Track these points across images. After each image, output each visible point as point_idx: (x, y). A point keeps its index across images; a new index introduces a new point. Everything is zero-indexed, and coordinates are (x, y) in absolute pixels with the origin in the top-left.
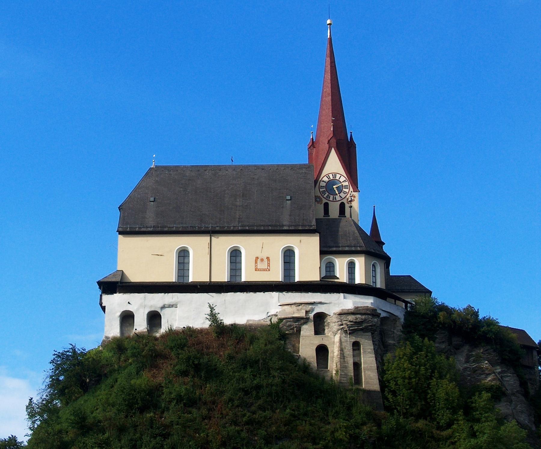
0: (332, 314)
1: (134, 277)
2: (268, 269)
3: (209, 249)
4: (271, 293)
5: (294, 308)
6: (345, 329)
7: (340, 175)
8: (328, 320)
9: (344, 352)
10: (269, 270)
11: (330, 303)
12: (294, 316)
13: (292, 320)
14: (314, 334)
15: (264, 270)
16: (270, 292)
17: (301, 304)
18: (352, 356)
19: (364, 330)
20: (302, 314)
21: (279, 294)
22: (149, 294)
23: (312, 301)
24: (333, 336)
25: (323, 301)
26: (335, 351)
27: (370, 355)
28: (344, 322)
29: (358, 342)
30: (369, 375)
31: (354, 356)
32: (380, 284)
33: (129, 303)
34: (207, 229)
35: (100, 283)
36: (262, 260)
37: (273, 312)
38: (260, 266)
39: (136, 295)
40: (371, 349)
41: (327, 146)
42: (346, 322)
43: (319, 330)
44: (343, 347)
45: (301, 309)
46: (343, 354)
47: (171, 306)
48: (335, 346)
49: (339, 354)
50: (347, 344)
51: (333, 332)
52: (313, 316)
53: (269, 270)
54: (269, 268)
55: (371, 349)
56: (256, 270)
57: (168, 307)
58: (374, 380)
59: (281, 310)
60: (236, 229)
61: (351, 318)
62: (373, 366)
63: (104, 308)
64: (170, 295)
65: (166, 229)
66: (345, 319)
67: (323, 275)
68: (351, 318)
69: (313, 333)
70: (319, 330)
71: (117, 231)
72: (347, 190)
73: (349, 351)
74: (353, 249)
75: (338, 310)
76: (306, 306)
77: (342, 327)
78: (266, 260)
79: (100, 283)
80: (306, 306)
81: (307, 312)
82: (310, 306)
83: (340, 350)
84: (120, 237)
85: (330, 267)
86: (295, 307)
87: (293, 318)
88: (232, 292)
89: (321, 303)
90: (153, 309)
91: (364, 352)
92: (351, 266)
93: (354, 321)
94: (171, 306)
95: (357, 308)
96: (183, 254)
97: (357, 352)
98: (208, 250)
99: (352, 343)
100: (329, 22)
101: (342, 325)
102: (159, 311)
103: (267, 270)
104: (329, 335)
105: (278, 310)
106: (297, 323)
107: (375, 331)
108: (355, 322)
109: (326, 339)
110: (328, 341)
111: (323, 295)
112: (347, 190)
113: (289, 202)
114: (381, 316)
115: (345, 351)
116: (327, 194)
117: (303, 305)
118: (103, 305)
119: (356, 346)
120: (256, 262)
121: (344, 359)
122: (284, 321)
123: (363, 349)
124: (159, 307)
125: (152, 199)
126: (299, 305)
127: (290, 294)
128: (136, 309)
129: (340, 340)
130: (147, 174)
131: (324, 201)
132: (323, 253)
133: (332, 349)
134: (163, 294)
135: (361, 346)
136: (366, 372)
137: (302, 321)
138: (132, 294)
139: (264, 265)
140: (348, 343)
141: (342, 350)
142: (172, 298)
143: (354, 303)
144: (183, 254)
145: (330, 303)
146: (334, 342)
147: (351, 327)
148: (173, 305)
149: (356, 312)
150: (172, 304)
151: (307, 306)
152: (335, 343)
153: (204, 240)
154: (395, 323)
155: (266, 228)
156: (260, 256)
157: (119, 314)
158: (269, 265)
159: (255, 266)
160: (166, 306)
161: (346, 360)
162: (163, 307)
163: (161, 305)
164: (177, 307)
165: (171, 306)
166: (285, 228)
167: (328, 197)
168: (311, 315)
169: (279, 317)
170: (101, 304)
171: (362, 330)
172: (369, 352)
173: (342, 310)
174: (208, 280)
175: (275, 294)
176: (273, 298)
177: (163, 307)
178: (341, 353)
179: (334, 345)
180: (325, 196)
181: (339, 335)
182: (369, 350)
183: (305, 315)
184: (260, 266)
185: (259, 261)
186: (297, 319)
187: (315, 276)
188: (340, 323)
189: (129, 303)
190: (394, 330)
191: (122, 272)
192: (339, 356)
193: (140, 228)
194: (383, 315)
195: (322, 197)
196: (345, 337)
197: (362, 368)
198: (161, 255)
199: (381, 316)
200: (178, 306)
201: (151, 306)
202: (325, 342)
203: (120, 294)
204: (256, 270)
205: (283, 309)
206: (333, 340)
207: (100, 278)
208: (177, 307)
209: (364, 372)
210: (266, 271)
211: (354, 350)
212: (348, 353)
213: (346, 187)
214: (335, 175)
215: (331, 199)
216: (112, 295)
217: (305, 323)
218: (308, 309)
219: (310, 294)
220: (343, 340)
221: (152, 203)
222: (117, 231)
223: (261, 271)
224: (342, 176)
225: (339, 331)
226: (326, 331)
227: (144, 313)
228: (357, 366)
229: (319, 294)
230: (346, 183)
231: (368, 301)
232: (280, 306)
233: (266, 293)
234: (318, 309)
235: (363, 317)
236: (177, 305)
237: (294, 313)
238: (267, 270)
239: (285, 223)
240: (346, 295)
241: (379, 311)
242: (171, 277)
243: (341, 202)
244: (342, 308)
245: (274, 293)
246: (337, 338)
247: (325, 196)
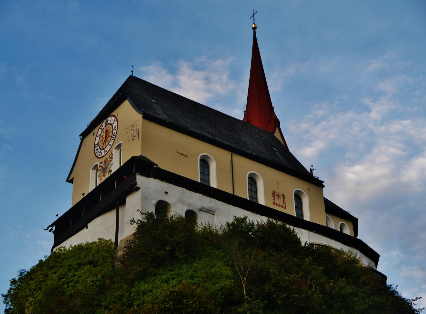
2: (284, 206)
4: (300, 229)
15: (281, 206)
33: (166, 193)
36: (278, 196)
39: (174, 186)
54: (285, 205)
56: (274, 203)
78: (282, 197)
90: (191, 208)
120: (273, 196)
127: (317, 235)
142: (211, 203)
148: (210, 211)
150: (210, 209)
153: (226, 155)
156: (277, 191)
157: (155, 202)
158: (284, 203)
160: (204, 209)
162: (201, 210)
163: (199, 206)
164: (214, 214)
165: (208, 211)
184: (277, 201)
185: (276, 196)
189: (166, 193)
198: (185, 156)
200: (216, 213)
208: (214, 214)
210: (283, 208)
223: (278, 206)
227: (182, 209)
236: (214, 212)
238: (284, 207)
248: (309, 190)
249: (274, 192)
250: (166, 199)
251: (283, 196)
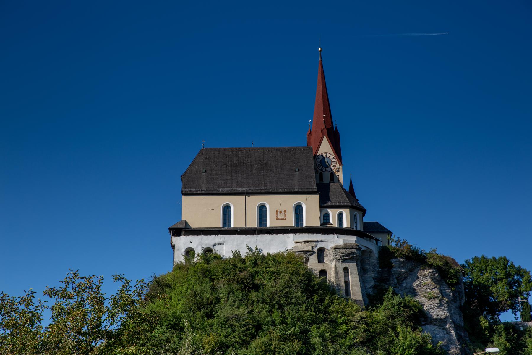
0: (329, 249)
1: (194, 225)
3: (245, 205)
4: (288, 234)
5: (304, 245)
6: (338, 259)
7: (330, 154)
8: (326, 252)
9: (339, 274)
10: (286, 219)
11: (328, 241)
12: (304, 250)
13: (302, 252)
14: (317, 262)
15: (282, 219)
16: (288, 234)
17: (308, 242)
18: (344, 277)
19: (351, 260)
20: (310, 249)
21: (293, 235)
22: (205, 236)
23: (316, 239)
24: (330, 264)
25: (323, 239)
26: (332, 274)
27: (355, 276)
28: (338, 254)
29: (348, 267)
30: (355, 289)
31: (345, 277)
32: (360, 228)
33: (191, 242)
34: (243, 192)
35: (170, 229)
36: (281, 212)
37: (289, 248)
38: (279, 216)
39: (196, 237)
40: (356, 272)
41: (321, 134)
42: (339, 253)
43: (320, 260)
44: (338, 271)
45: (309, 245)
46: (338, 275)
47: (219, 244)
48: (332, 270)
49: (335, 275)
50: (340, 269)
51: (330, 261)
52: (316, 250)
53: (286, 219)
54: (285, 217)
55: (356, 272)
56: (277, 219)
57: (218, 245)
58: (358, 293)
59: (295, 246)
60: (263, 191)
61: (343, 251)
62: (357, 283)
63: (173, 247)
64: (219, 236)
65: (215, 192)
66: (338, 252)
67: (322, 222)
68: (343, 251)
69: (317, 261)
70: (320, 260)
71: (181, 193)
72: (335, 164)
73: (342, 274)
74: (342, 204)
75: (333, 245)
76: (312, 243)
77: (336, 257)
79: (170, 229)
80: (312, 243)
81: (312, 248)
82: (315, 243)
83: (336, 273)
84: (183, 196)
85: (326, 217)
86: (305, 244)
87: (303, 251)
88: (261, 234)
89: (322, 241)
90: (207, 246)
91: (351, 274)
92: (340, 216)
93: (345, 253)
94: (219, 244)
95: (346, 244)
96: (227, 209)
97: (346, 274)
98: (244, 206)
99: (343, 268)
100: (320, 49)
101: (336, 256)
102: (212, 247)
103: (285, 219)
104: (328, 262)
105: (293, 246)
106: (306, 255)
107: (358, 259)
108: (346, 254)
109: (326, 265)
110: (327, 266)
111: (323, 235)
112: (335, 164)
113: (297, 173)
114: (362, 250)
115: (339, 273)
116: (322, 167)
117: (310, 242)
118: (173, 244)
119: (346, 269)
120: (277, 214)
121: (338, 279)
122: (310, 253)
123: (351, 272)
124: (212, 245)
125: (204, 171)
126: (307, 243)
127: (301, 235)
128: (196, 246)
129: (336, 266)
130: (199, 153)
131: (320, 172)
132: (322, 207)
133: (330, 272)
134: (214, 236)
135: (349, 270)
136: (353, 287)
137: (310, 253)
138: (193, 236)
139: (282, 216)
140: (341, 268)
141: (337, 273)
142: (221, 239)
143: (344, 240)
144: (227, 209)
145: (328, 241)
146: (331, 267)
147: (342, 257)
148: (221, 243)
149: (346, 247)
151: (313, 243)
152: (332, 268)
154: (370, 254)
155: (283, 191)
156: (280, 209)
158: (285, 215)
159: (276, 216)
160: (216, 244)
161: (339, 280)
162: (214, 245)
163: (213, 243)
164: (224, 245)
166: (297, 190)
167: (322, 169)
168: (315, 249)
169: (294, 251)
170: (171, 244)
171: (350, 259)
172: (355, 274)
173: (336, 246)
174: (245, 226)
175: (291, 236)
176: (289, 238)
177: (214, 245)
178: (336, 275)
179: (331, 269)
180: (320, 168)
181: (335, 263)
182: (355, 273)
183: (311, 249)
184: (279, 216)
186: (307, 252)
187: (316, 223)
188: (335, 254)
189: (191, 242)
190: (369, 259)
191: (185, 221)
192: (335, 277)
193: (197, 191)
194: (363, 248)
195: (317, 169)
196: (339, 264)
197: (350, 285)
198: (212, 209)
199: (362, 250)
201: (206, 245)
202: (325, 267)
203: (185, 236)
204: (277, 219)
205: (296, 245)
206: (330, 266)
207: (170, 226)
209: (352, 287)
211: (345, 273)
212: (341, 275)
213: (334, 162)
214: (327, 154)
215: (324, 170)
216: (179, 237)
217: (311, 255)
218: (313, 245)
219: (314, 235)
220: (337, 266)
221: (204, 173)
222: (181, 193)
223: (280, 219)
224: (331, 155)
225: (335, 260)
226: (325, 260)
228: (347, 283)
229: (320, 235)
230: (334, 160)
231: (352, 239)
232: (295, 244)
233: (284, 234)
234: (320, 245)
235: (351, 250)
237: (303, 248)
238: (285, 219)
239: (296, 187)
240: (339, 235)
241: (360, 246)
242: (219, 224)
243: (331, 172)
244: (336, 244)
245: (290, 234)
246: (333, 265)
247: (320, 168)
248: (306, 199)
249: (277, 211)
250: (191, 246)
251: (285, 211)
